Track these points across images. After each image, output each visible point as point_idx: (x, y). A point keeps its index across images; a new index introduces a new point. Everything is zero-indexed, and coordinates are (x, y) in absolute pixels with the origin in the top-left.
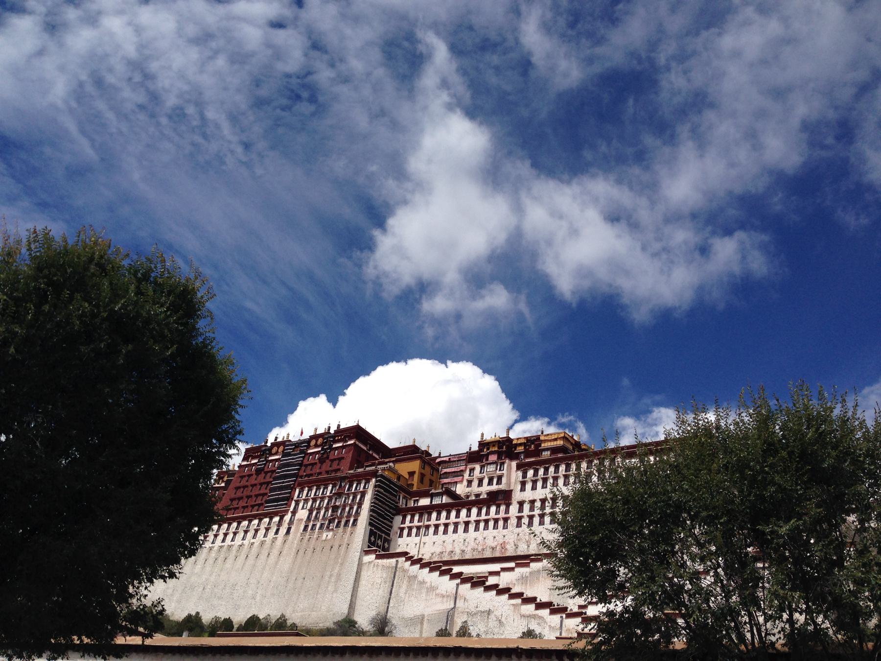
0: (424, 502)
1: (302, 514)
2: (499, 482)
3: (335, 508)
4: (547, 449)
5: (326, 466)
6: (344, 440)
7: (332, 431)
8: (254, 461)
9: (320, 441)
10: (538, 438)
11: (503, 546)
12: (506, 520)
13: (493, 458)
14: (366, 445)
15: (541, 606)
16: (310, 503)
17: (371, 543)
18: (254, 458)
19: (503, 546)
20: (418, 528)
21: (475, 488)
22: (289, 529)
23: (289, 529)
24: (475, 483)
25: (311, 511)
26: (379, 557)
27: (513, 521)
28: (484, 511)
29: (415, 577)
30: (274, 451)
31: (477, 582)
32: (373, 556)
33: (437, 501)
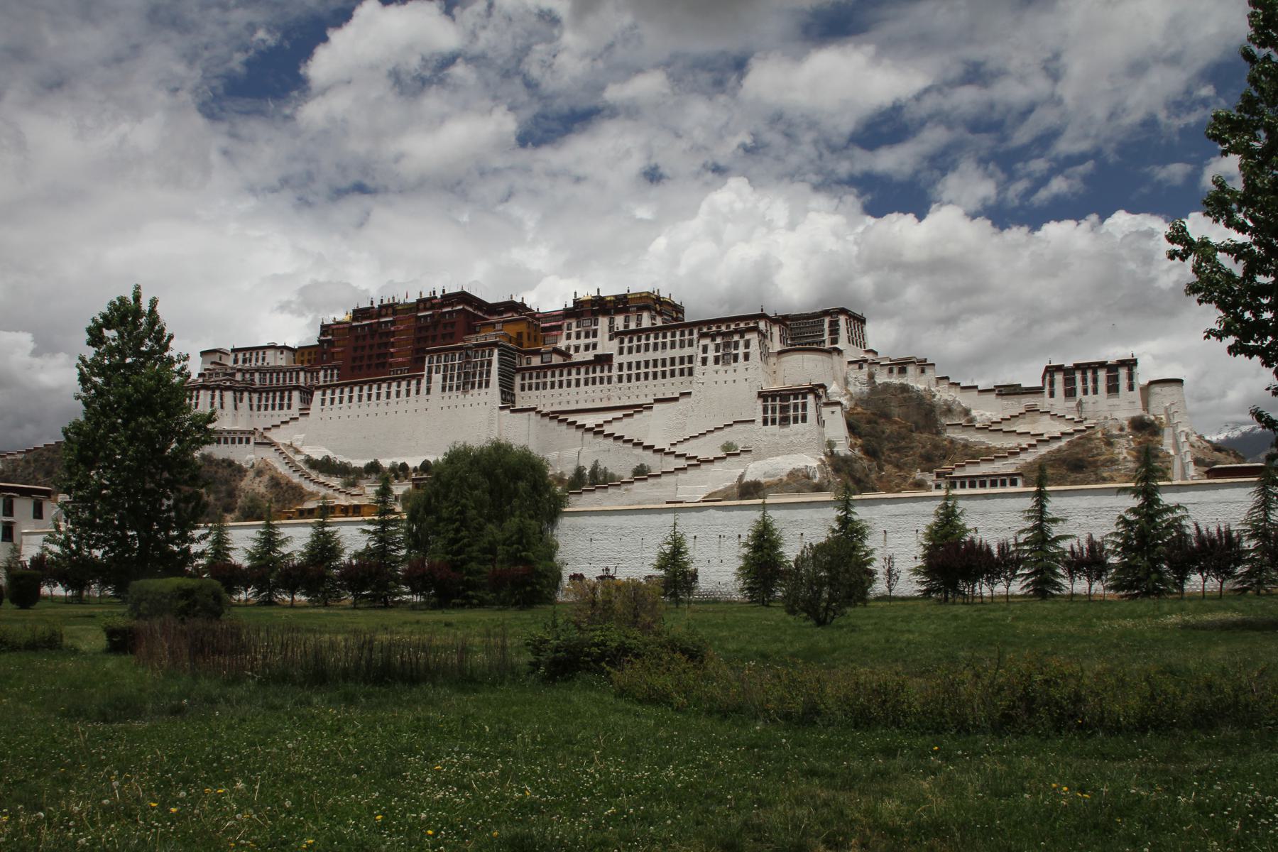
0: (536, 361)
1: (437, 378)
2: (595, 335)
3: (467, 374)
6: (452, 305)
7: (438, 295)
9: (428, 305)
10: (625, 296)
14: (471, 306)
17: (504, 400)
21: (573, 342)
24: (573, 335)
26: (512, 411)
27: (615, 379)
30: (384, 312)
31: (597, 431)
32: (507, 412)
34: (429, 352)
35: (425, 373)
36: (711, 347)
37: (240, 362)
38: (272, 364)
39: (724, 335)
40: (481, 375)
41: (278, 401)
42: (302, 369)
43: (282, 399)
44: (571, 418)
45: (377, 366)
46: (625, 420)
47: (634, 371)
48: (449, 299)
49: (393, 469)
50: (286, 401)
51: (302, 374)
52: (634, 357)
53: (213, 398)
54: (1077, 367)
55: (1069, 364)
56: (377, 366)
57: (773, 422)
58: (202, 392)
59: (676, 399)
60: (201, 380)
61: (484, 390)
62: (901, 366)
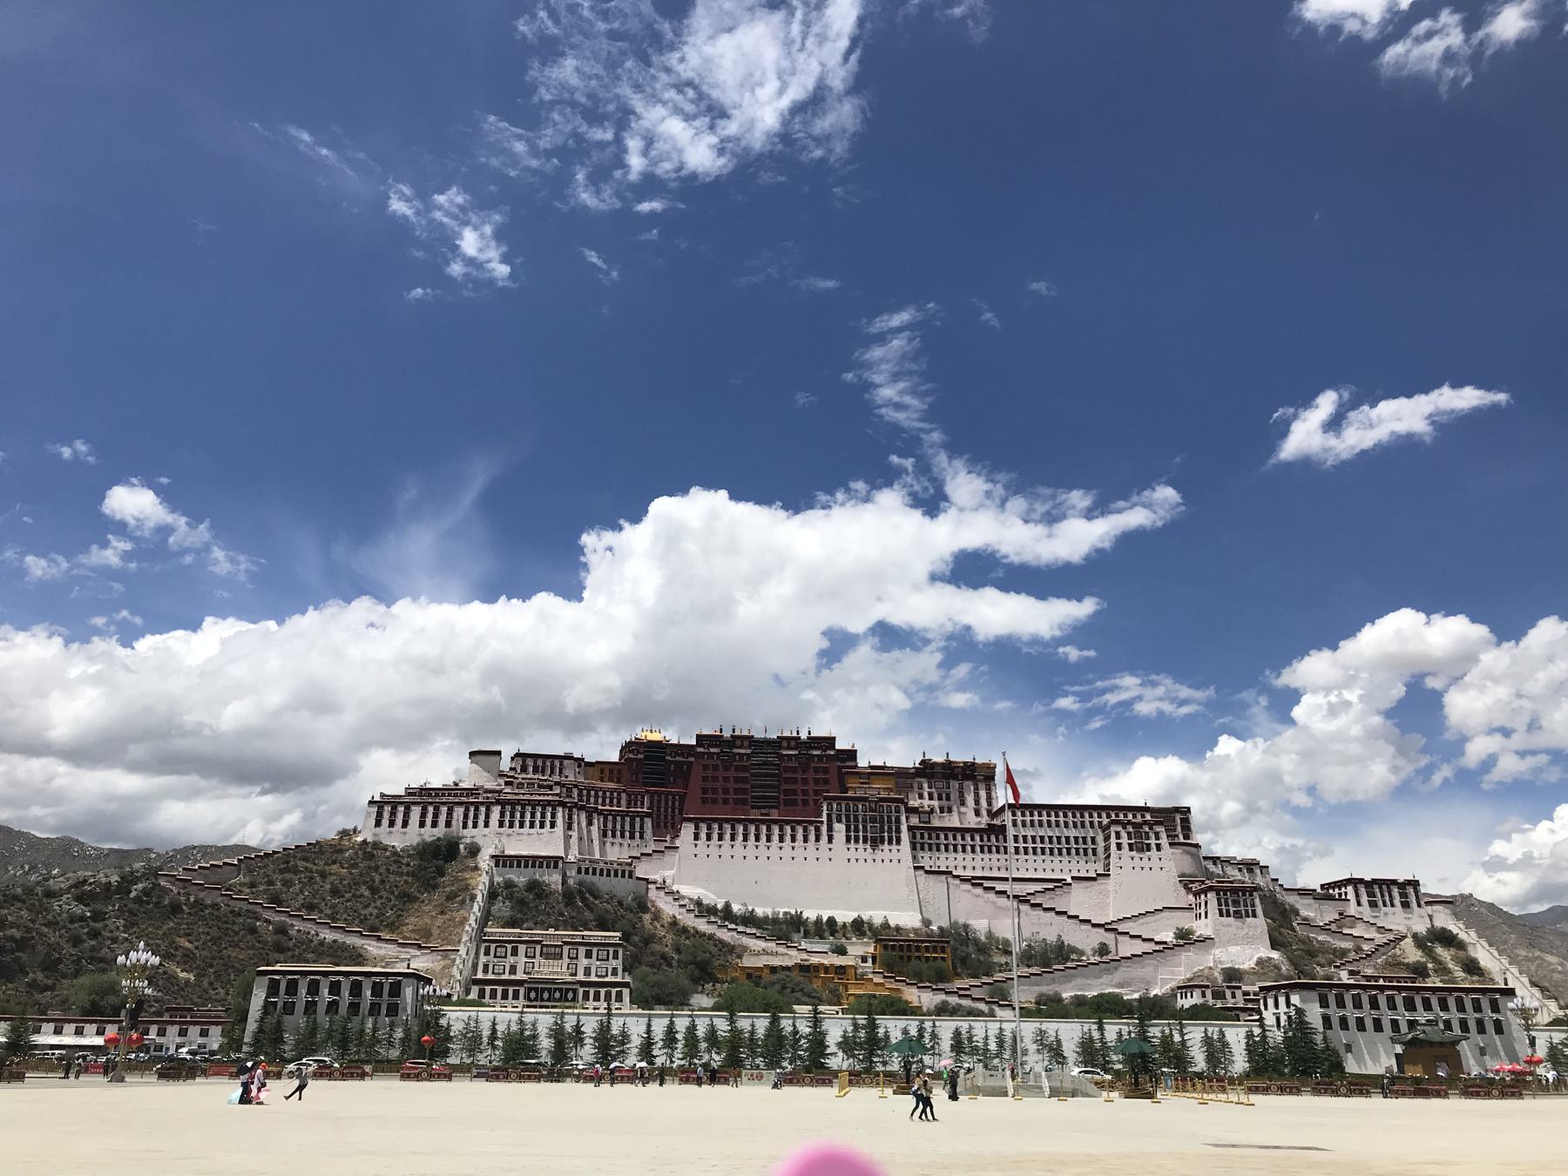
1: (839, 828)
2: (948, 798)
5: (811, 775)
7: (804, 736)
9: (793, 743)
15: (1095, 926)
18: (710, 746)
22: (830, 840)
23: (830, 840)
26: (927, 872)
30: (738, 743)
34: (826, 798)
35: (824, 819)
36: (1124, 835)
38: (571, 778)
39: (1135, 825)
40: (890, 828)
41: (627, 827)
43: (632, 826)
45: (737, 801)
46: (1048, 895)
47: (1030, 845)
48: (815, 742)
49: (819, 920)
54: (1374, 881)
55: (1368, 878)
56: (737, 801)
57: (1228, 915)
59: (1093, 879)
61: (894, 847)
62: (1250, 866)
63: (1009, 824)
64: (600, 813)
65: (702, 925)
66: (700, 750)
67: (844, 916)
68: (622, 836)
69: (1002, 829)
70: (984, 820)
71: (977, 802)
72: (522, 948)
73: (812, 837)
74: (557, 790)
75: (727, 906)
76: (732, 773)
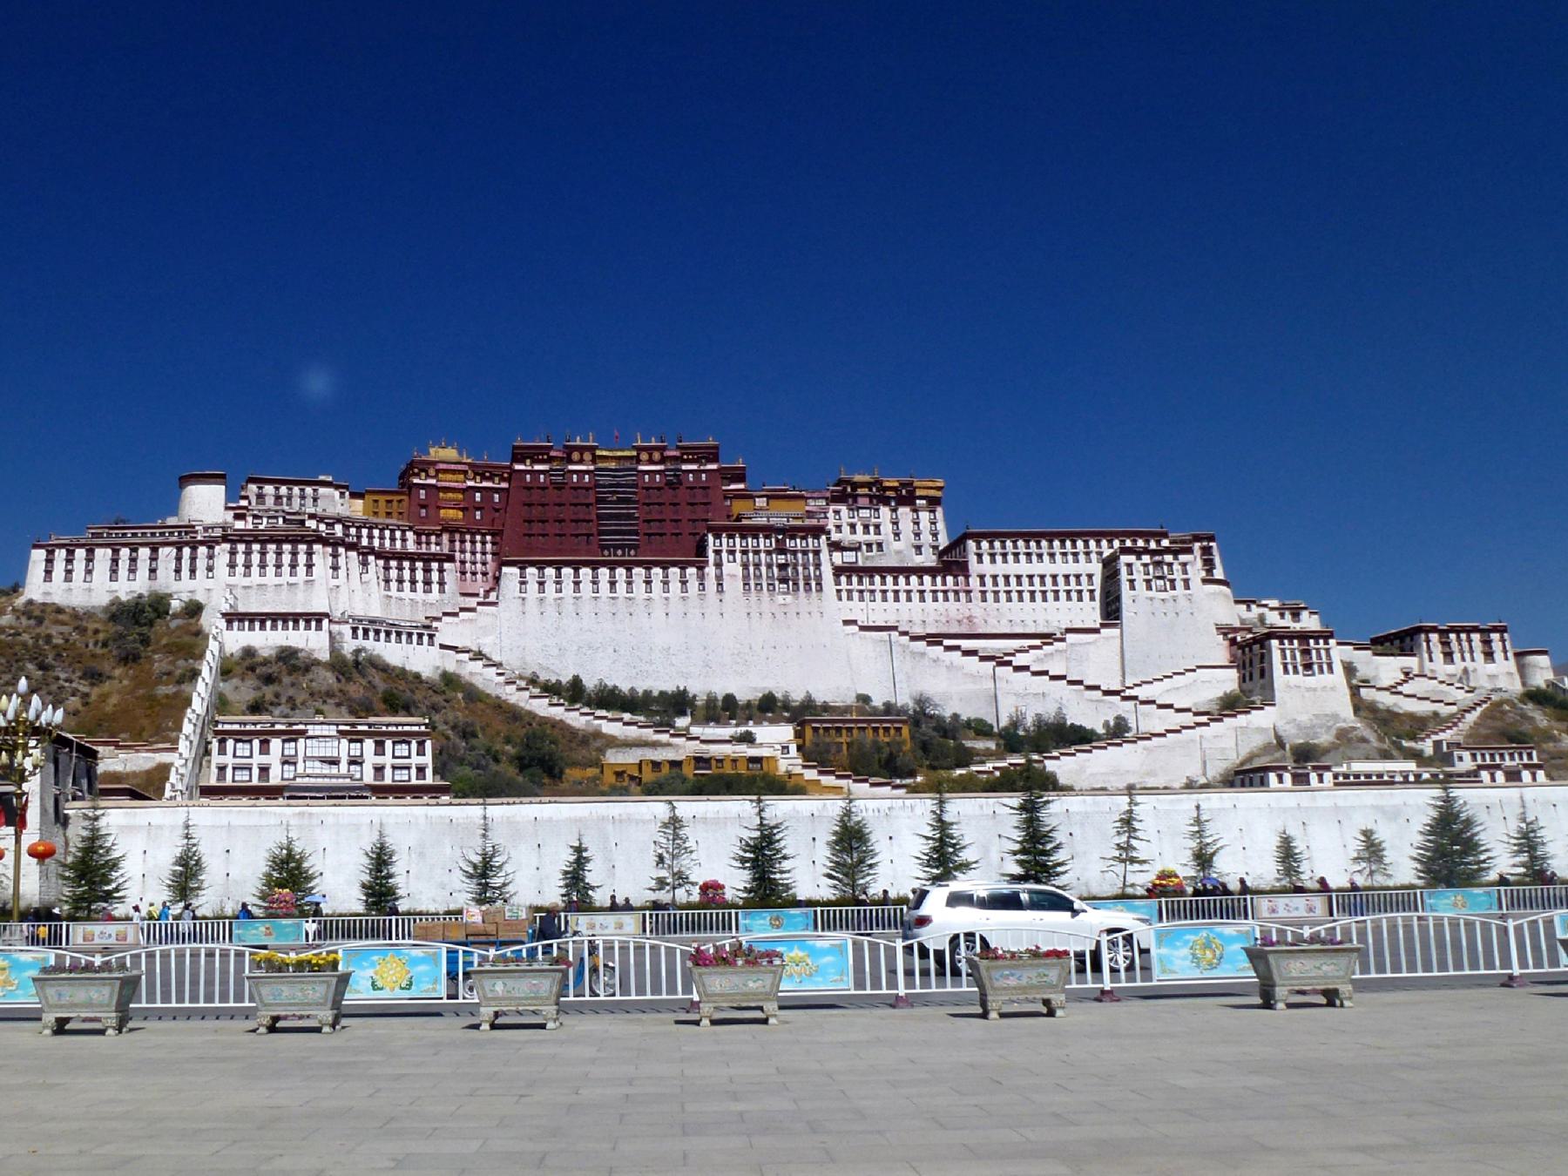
1: (732, 569)
2: (878, 532)
4: (921, 498)
5: (682, 495)
8: (537, 467)
9: (656, 456)
11: (970, 619)
12: (968, 592)
13: (863, 501)
16: (738, 555)
18: (534, 461)
19: (970, 619)
20: (861, 592)
21: (845, 536)
25: (745, 566)
26: (863, 628)
27: (976, 595)
28: (939, 579)
29: (923, 654)
30: (576, 456)
33: (849, 557)
37: (270, 502)
42: (411, 529)
43: (427, 570)
44: (966, 644)
49: (711, 701)
50: (435, 576)
51: (410, 535)
52: (1000, 568)
53: (335, 556)
58: (317, 547)
60: (240, 525)
63: (973, 559)
64: (378, 556)
65: (542, 707)
66: (518, 467)
67: (746, 690)
68: (413, 590)
69: (961, 569)
70: (928, 559)
71: (917, 535)
72: (276, 743)
73: (693, 584)
74: (312, 524)
75: (576, 682)
76: (567, 496)
